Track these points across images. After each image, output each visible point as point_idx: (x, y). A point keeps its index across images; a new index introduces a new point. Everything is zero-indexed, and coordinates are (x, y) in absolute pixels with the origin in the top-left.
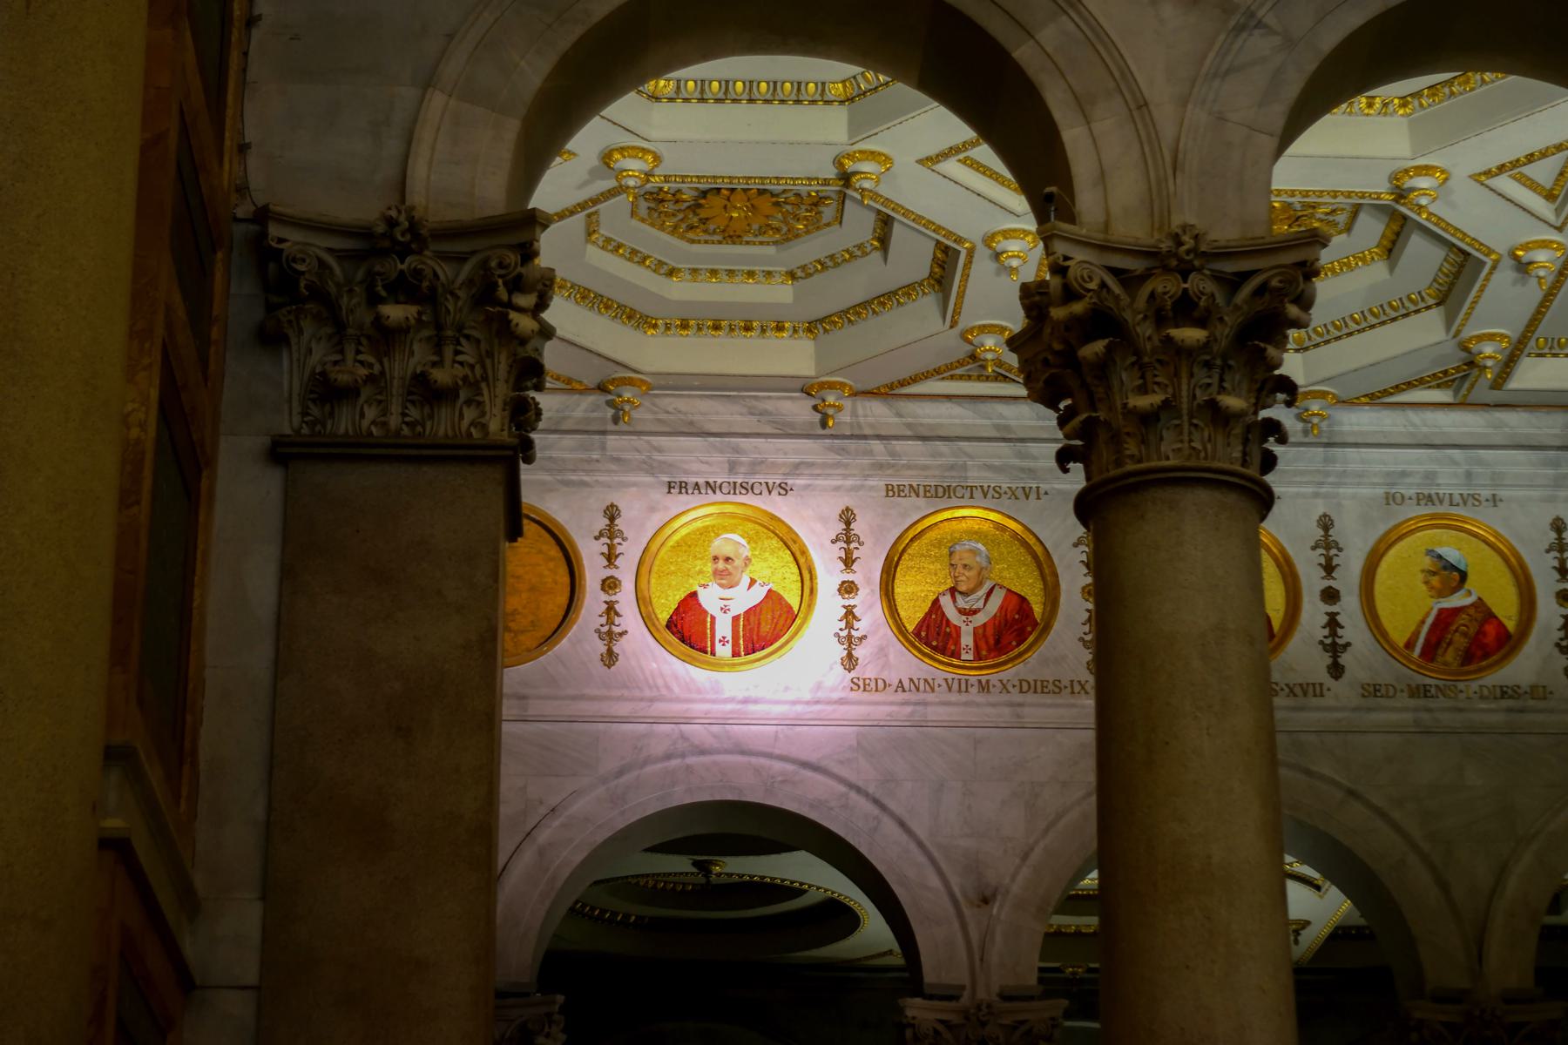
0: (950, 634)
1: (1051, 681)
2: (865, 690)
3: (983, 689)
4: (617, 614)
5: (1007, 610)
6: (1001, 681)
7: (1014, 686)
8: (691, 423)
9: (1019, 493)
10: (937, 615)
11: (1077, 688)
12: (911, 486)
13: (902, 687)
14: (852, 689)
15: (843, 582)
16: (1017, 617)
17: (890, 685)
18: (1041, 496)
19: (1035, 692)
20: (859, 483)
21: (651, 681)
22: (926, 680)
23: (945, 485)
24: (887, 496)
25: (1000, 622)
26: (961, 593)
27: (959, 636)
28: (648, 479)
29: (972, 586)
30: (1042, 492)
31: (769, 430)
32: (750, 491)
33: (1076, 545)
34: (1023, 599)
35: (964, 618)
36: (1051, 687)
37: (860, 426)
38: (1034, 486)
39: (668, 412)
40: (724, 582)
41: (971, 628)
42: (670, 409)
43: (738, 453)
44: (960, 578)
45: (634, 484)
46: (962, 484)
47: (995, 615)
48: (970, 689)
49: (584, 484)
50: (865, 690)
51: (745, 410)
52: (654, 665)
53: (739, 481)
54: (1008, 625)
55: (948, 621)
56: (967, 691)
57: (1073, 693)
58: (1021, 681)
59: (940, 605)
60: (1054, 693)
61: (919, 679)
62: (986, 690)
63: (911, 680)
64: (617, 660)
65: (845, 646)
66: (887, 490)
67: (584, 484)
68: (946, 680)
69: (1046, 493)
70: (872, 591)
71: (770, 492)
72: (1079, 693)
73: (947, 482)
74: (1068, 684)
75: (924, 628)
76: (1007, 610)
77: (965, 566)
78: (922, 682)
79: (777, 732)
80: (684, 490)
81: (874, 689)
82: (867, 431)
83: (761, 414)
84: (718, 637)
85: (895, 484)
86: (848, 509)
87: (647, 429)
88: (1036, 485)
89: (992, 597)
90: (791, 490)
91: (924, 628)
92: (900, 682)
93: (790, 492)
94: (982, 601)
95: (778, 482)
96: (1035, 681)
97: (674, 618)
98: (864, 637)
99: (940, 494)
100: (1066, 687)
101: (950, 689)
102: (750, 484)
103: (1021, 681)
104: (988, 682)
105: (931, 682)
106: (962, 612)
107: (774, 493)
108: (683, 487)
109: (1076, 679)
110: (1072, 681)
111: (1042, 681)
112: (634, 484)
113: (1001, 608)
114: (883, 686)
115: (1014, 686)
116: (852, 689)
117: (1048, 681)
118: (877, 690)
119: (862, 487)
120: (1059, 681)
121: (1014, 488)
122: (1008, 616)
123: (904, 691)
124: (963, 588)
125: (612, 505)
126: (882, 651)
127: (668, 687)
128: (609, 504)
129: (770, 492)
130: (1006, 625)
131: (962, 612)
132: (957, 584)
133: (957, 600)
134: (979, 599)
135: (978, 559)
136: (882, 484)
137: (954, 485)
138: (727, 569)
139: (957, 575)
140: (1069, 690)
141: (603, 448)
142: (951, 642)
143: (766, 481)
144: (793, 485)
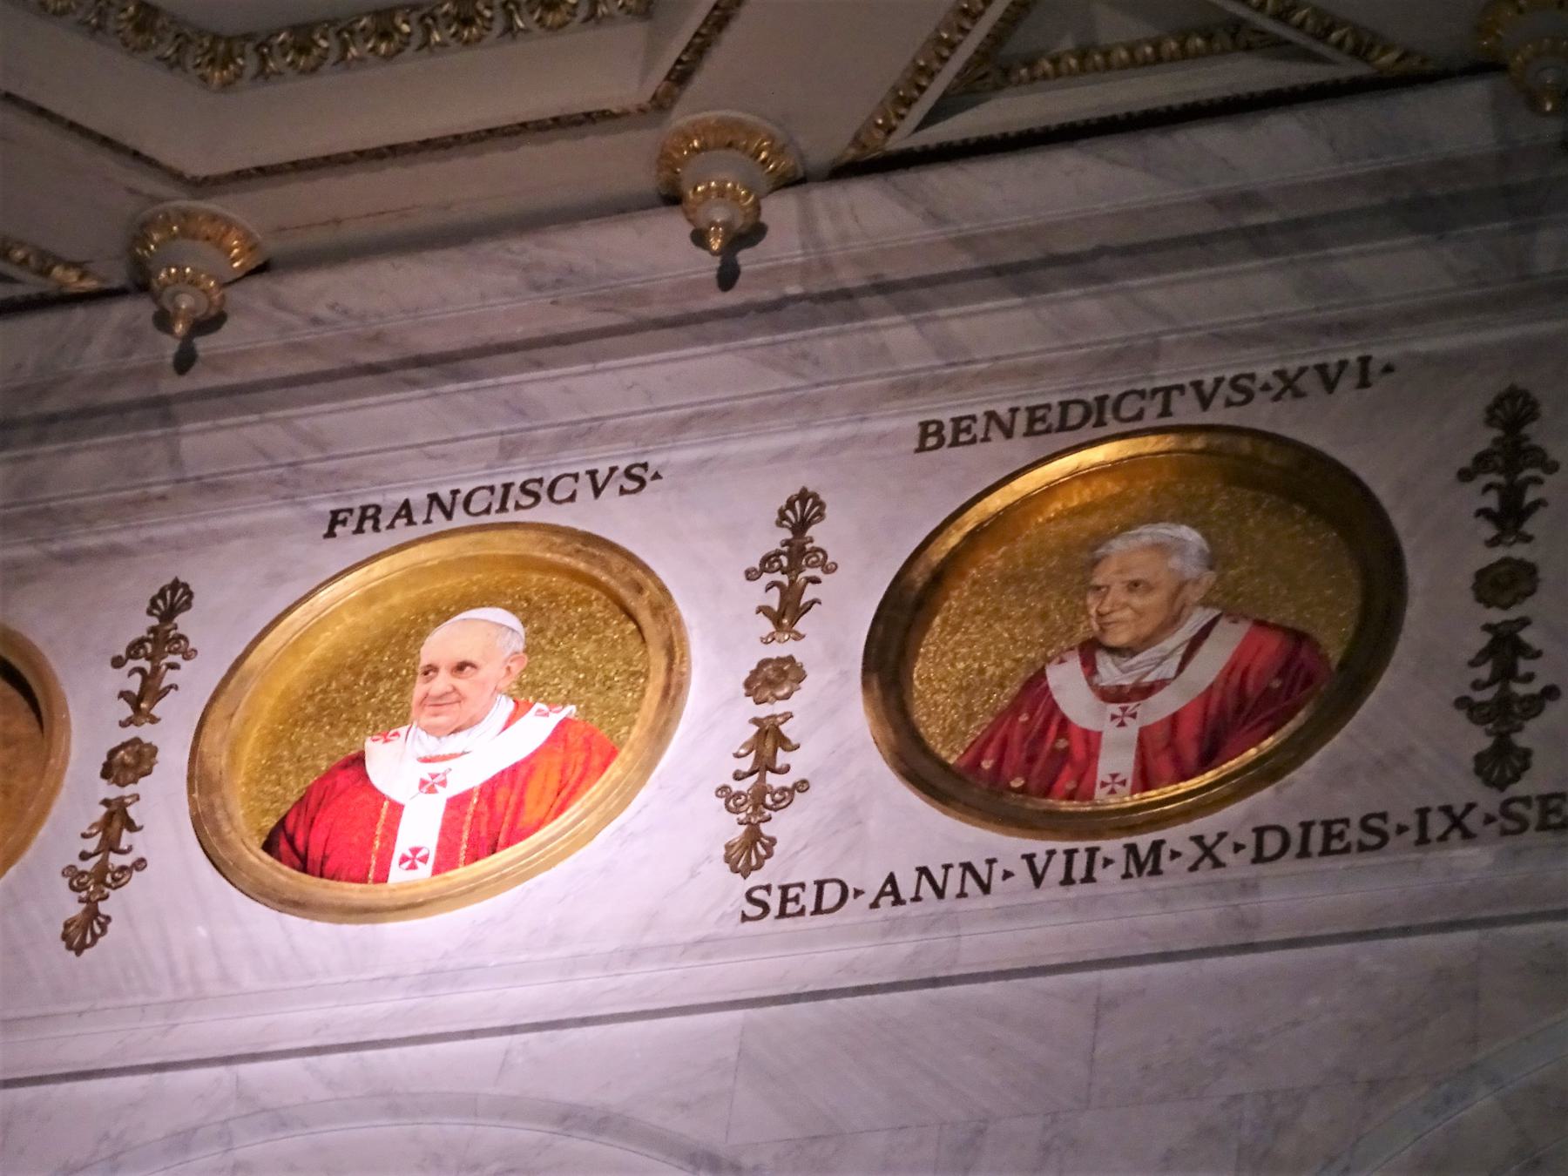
0: (1066, 755)
1: (1355, 822)
2: (783, 914)
3: (1140, 868)
4: (131, 826)
5: (1245, 674)
6: (1198, 839)
7: (1238, 848)
8: (378, 338)
9: (1309, 382)
10: (1031, 715)
11: (1437, 824)
12: (991, 415)
13: (895, 891)
14: (745, 918)
15: (764, 663)
16: (1276, 684)
17: (858, 893)
18: (1371, 378)
19: (1304, 853)
20: (846, 430)
21: (183, 973)
22: (967, 867)
23: (1090, 396)
24: (922, 448)
25: (1222, 702)
26: (1113, 651)
27: (1092, 755)
28: (285, 513)
29: (1146, 629)
30: (1374, 367)
31: (578, 319)
32: (544, 497)
33: (1465, 475)
34: (1299, 638)
35: (1115, 708)
36: (1354, 834)
37: (827, 267)
38: (1353, 357)
39: (316, 321)
40: (441, 720)
41: (1133, 728)
42: (322, 311)
43: (522, 413)
44: (1116, 616)
45: (238, 534)
46: (1139, 387)
47: (1211, 687)
48: (1098, 872)
49: (115, 551)
50: (783, 914)
51: (513, 279)
52: (202, 932)
53: (519, 480)
54: (1248, 707)
55: (1064, 722)
56: (1089, 878)
57: (1423, 840)
58: (1260, 832)
59: (1047, 688)
60: (1363, 848)
61: (947, 867)
62: (1149, 867)
63: (923, 871)
64: (104, 930)
65: (742, 816)
66: (924, 435)
67: (115, 551)
68: (1029, 858)
69: (1388, 369)
70: (844, 674)
71: (597, 492)
72: (1443, 838)
73: (1096, 387)
74: (1412, 821)
75: (994, 744)
76: (1245, 674)
77: (1134, 586)
78: (956, 873)
79: (507, 1052)
80: (368, 524)
81: (810, 907)
82: (850, 278)
83: (558, 283)
84: (402, 847)
85: (946, 418)
86: (804, 496)
87: (259, 372)
88: (1360, 353)
89: (1206, 648)
90: (657, 476)
91: (990, 751)
92: (891, 879)
93: (650, 484)
94: (1175, 661)
95: (623, 465)
96: (1306, 827)
97: (290, 824)
98: (802, 786)
99: (1072, 422)
100: (1401, 829)
101: (1038, 880)
102: (546, 484)
103: (1260, 832)
104: (1156, 846)
105: (983, 871)
106: (1111, 695)
107: (610, 491)
108: (370, 517)
109: (1435, 803)
110: (1423, 813)
111: (1327, 825)
112: (238, 534)
113: (1231, 668)
114: (837, 899)
115: (1238, 848)
116: (745, 918)
117: (1346, 821)
118: (818, 910)
119: (852, 440)
120: (1383, 816)
121: (1291, 373)
122: (1250, 683)
123: (898, 901)
124: (1119, 637)
125: (176, 585)
126: (850, 813)
127: (225, 978)
128: (168, 581)
129: (597, 492)
130: (1239, 709)
131: (1111, 695)
132: (1103, 630)
133: (1100, 669)
134: (1164, 658)
135: (1175, 562)
136: (912, 423)
137: (1114, 393)
138: (455, 689)
139: (1106, 609)
140: (1413, 835)
141: (175, 460)
142: (1068, 769)
143: (591, 467)
144: (664, 466)
